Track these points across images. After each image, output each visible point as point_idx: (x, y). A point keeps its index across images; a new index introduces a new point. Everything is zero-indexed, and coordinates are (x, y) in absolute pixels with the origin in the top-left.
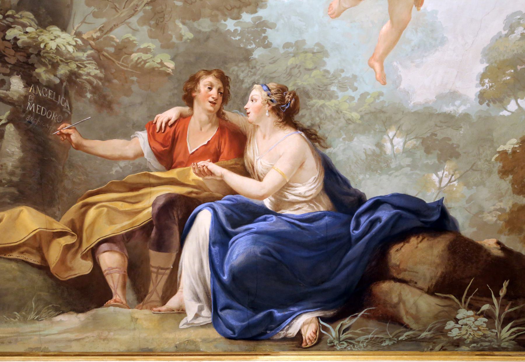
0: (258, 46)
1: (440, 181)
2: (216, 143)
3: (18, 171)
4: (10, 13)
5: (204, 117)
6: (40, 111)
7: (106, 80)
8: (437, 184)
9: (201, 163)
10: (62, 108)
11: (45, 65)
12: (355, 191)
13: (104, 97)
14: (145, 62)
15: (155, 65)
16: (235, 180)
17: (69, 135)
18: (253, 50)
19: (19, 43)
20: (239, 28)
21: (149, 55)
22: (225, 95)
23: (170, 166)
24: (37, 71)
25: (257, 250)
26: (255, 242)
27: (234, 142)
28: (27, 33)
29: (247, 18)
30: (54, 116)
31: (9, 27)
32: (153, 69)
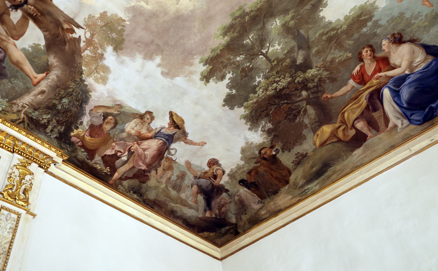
0: (377, 29)
2: (378, 66)
3: (316, 117)
5: (369, 62)
7: (331, 73)
9: (375, 76)
10: (320, 90)
11: (310, 82)
13: (333, 78)
14: (341, 60)
15: (345, 58)
16: (391, 73)
17: (327, 97)
18: (376, 31)
19: (300, 82)
20: (368, 29)
21: (342, 57)
22: (373, 51)
23: (365, 84)
25: (412, 89)
26: (409, 87)
27: (384, 62)
29: (369, 24)
31: (295, 79)
32: (345, 60)
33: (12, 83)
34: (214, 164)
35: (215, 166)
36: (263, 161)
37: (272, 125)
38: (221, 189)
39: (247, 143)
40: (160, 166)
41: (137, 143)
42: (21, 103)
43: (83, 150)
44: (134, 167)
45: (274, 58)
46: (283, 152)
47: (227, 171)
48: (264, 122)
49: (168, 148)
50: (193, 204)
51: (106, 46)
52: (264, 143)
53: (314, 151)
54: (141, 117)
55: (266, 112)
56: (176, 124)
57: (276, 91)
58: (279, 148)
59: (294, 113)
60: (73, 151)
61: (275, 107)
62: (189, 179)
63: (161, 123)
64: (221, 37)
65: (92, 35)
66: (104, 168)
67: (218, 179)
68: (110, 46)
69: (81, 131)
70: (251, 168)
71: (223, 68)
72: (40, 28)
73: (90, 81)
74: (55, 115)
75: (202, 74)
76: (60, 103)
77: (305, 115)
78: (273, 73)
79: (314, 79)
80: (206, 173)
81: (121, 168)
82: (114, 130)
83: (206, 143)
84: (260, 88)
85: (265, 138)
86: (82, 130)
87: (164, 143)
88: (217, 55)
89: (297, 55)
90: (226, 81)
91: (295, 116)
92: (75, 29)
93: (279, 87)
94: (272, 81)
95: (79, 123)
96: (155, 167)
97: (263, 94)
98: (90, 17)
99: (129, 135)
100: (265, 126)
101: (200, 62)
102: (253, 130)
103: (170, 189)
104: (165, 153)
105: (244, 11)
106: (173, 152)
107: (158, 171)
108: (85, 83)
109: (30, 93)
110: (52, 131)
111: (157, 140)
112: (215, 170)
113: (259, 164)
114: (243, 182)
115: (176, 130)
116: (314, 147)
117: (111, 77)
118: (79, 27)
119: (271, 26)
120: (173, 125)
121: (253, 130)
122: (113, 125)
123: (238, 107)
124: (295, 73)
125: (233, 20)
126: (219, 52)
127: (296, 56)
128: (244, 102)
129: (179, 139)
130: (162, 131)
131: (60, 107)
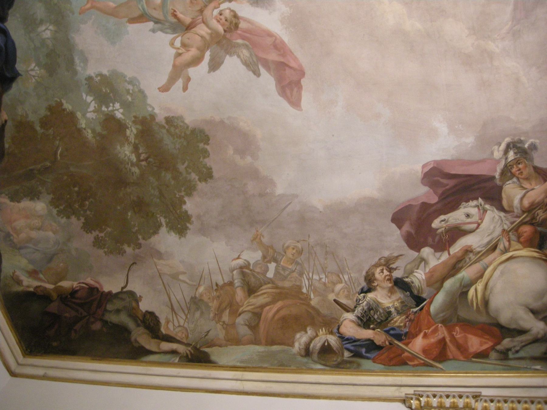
1: (32, 70)
8: (29, 69)
12: (7, 14)
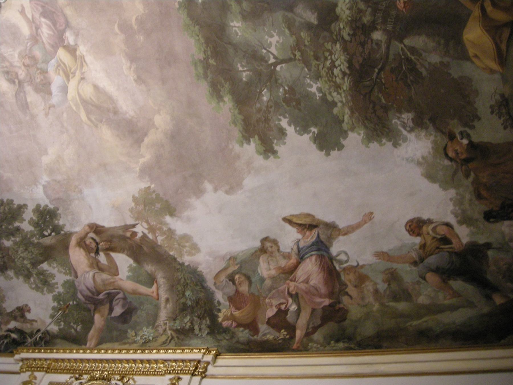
4: (335, 37)
6: (392, 22)
10: (386, 7)
11: (361, 17)
24: (366, 22)
28: (344, 28)
30: (393, 13)
33: (144, 310)
34: (420, 228)
35: (424, 228)
36: (471, 165)
37: (408, 111)
38: (475, 252)
39: (419, 164)
40: (346, 285)
41: (291, 280)
42: (162, 322)
43: (241, 329)
44: (313, 310)
45: (290, 52)
46: (473, 127)
47: (452, 220)
48: (396, 120)
49: (331, 259)
50: (454, 301)
51: (163, 220)
52: (434, 142)
53: (505, 80)
54: (263, 250)
55: (377, 107)
56: (308, 225)
57: (349, 75)
58: (461, 129)
59: (407, 69)
60: (232, 337)
61: (376, 91)
62: (408, 274)
63: (290, 238)
64: (221, 104)
65: (147, 222)
66: (278, 334)
67: (454, 241)
68: (166, 217)
69: (225, 312)
70: (471, 189)
71: (268, 124)
72: (119, 252)
73: (187, 259)
74: (192, 313)
75: (258, 152)
76: (187, 299)
77: (421, 55)
78: (314, 64)
79: (359, 9)
80: (423, 246)
81: (299, 321)
82: (253, 285)
83: (372, 213)
84: (330, 93)
85: (426, 136)
86: (225, 310)
87: (321, 257)
88: (244, 120)
89: (301, 17)
90: (290, 130)
91: (413, 69)
92: (134, 230)
93: (344, 67)
94: (327, 74)
95: (217, 305)
96: (340, 291)
97: (343, 95)
98: (131, 210)
99: (273, 278)
100: (404, 123)
101: (242, 145)
102: (401, 142)
103: (392, 304)
104: (335, 267)
105: (200, 61)
106: (343, 257)
107: (350, 293)
108: (186, 264)
109: (160, 308)
110: (200, 329)
111: (308, 260)
112: (431, 232)
113: (472, 174)
114: (489, 216)
115: (315, 232)
116: (497, 76)
117: (196, 239)
118: (134, 226)
119: (237, 34)
120: (304, 229)
121: (401, 142)
122: (247, 283)
123: (345, 138)
124: (331, 33)
125: (206, 80)
126: (240, 117)
127: (301, 20)
128: (341, 127)
129: (331, 239)
130: (301, 245)
131: (189, 303)
